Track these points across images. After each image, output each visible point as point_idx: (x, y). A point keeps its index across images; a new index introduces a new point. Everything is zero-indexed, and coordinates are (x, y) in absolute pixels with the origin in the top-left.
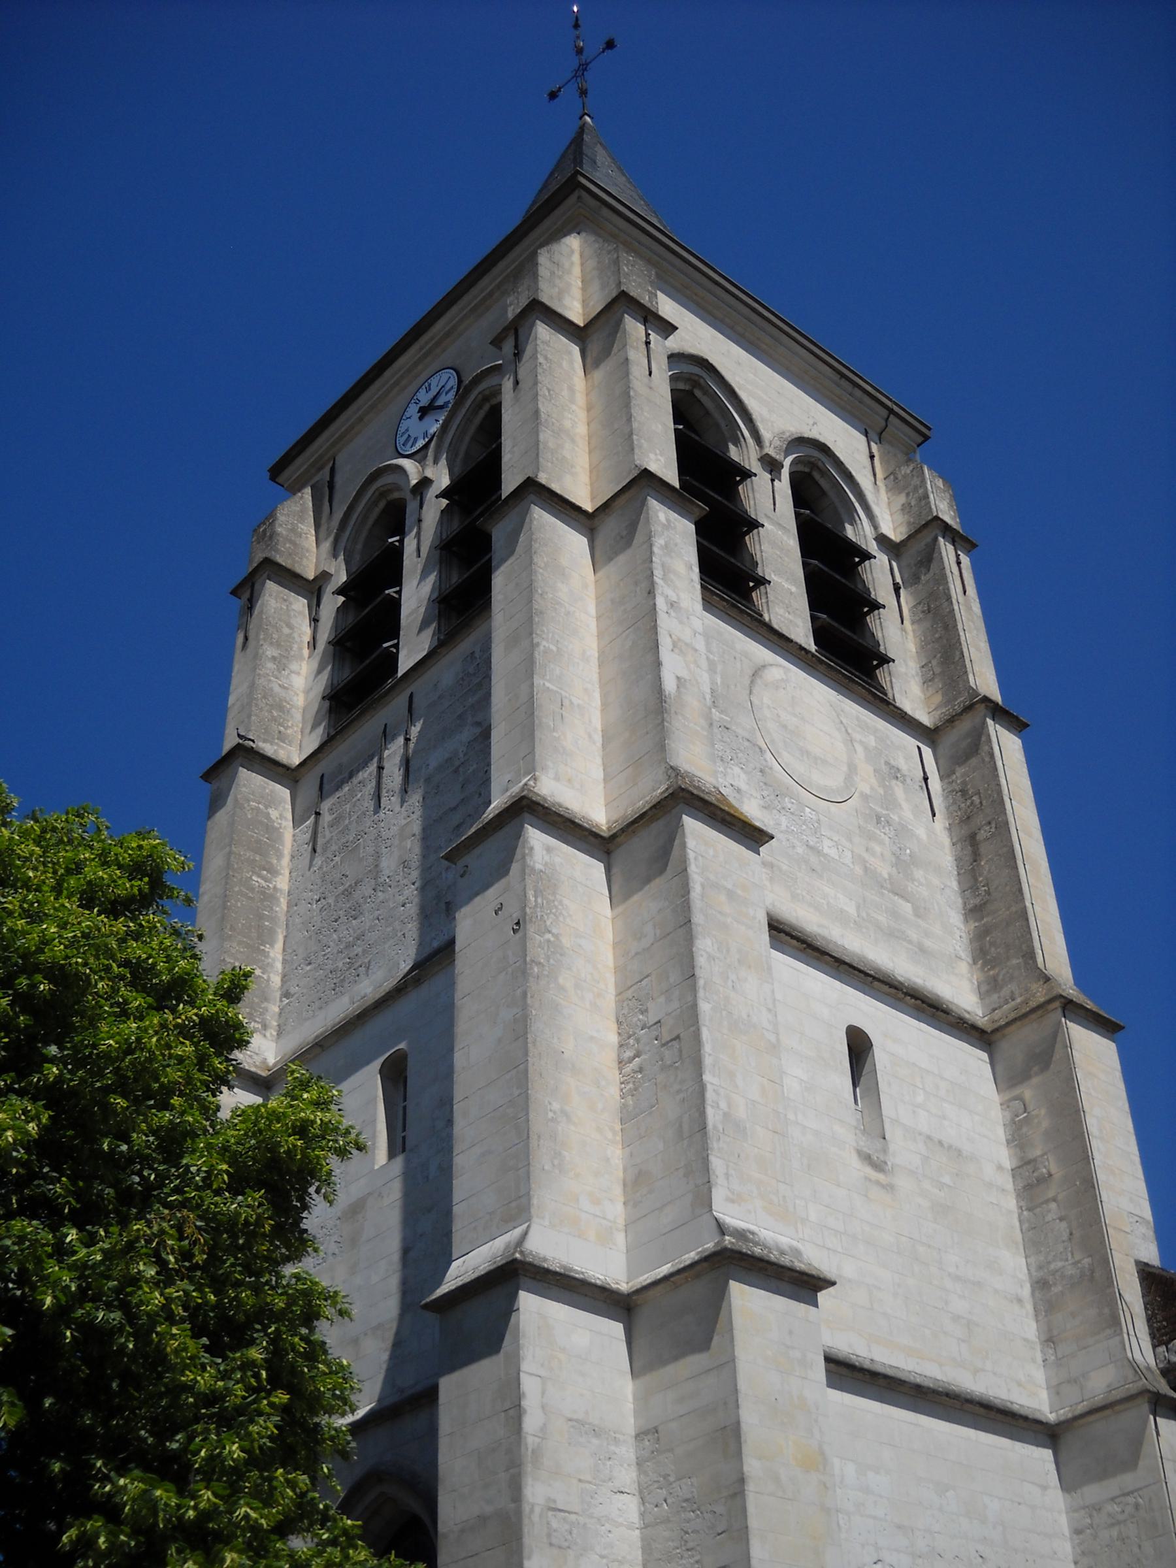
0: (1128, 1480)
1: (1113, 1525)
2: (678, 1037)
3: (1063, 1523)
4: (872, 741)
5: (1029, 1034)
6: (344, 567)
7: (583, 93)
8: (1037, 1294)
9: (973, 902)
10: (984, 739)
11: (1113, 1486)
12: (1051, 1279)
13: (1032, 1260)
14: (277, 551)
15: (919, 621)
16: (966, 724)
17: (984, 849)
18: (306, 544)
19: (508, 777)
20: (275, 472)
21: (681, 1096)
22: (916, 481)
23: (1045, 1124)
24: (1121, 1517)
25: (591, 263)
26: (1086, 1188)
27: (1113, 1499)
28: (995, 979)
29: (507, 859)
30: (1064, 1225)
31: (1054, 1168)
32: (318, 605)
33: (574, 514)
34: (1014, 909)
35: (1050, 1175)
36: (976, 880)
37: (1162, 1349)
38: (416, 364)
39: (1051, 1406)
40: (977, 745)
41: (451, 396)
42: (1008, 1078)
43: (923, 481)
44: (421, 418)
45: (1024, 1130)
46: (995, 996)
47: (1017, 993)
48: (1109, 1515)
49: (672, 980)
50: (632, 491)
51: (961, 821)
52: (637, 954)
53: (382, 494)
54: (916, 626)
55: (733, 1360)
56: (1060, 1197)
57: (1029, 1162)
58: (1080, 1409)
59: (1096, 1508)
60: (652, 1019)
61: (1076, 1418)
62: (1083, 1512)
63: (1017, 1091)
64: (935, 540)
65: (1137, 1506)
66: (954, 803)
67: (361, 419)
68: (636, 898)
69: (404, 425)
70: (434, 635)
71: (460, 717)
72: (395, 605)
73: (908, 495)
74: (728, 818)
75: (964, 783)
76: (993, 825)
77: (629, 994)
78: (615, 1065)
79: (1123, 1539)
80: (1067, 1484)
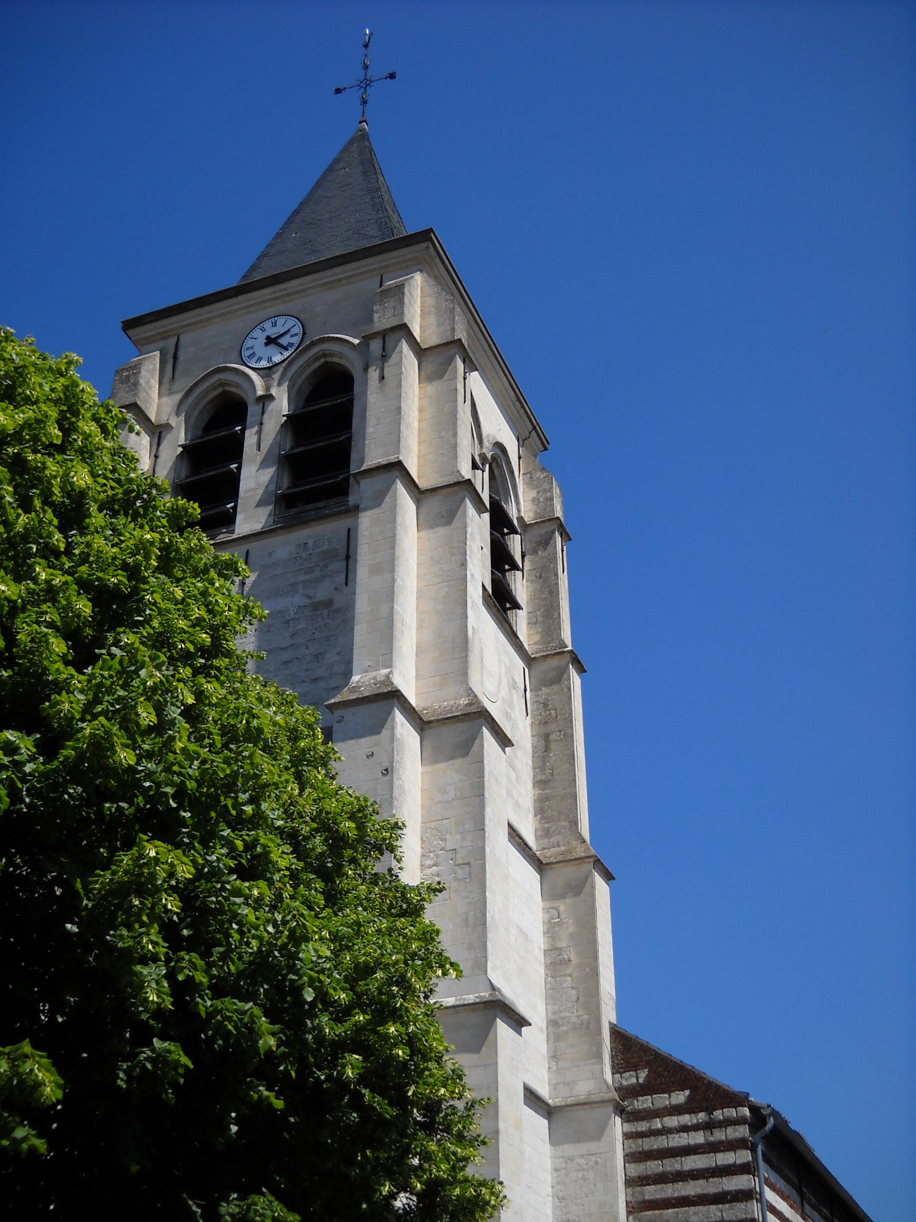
0: (593, 1146)
1: (579, 1170)
2: (468, 864)
3: (548, 1163)
4: (507, 661)
5: (569, 872)
6: (183, 425)
7: (365, 102)
8: (550, 1028)
9: (540, 777)
10: (565, 676)
11: (583, 1148)
12: (560, 1021)
13: (549, 1007)
14: (139, 397)
15: (532, 581)
16: (555, 662)
17: (553, 746)
18: (152, 395)
19: (369, 663)
20: (128, 325)
21: (469, 900)
22: (546, 486)
23: (571, 929)
24: (585, 1167)
25: (430, 301)
26: (594, 974)
27: (582, 1156)
28: (548, 830)
29: (378, 725)
30: (574, 992)
31: (572, 957)
32: (159, 445)
33: (413, 488)
34: (568, 791)
35: (570, 961)
36: (545, 764)
37: (618, 1076)
38: (266, 301)
39: (550, 1094)
40: (560, 678)
41: (296, 340)
42: (550, 894)
43: (551, 488)
44: (266, 344)
45: (557, 929)
46: (546, 841)
47: (561, 843)
48: (578, 1164)
49: (466, 827)
50: (456, 489)
51: (540, 723)
52: (440, 802)
53: (222, 384)
54: (529, 584)
55: (496, 1064)
56: (574, 975)
57: (556, 949)
58: (570, 1101)
59: (571, 1159)
60: (449, 847)
61: (567, 1106)
62: (561, 1160)
63: (555, 904)
64: (553, 532)
65: (596, 1163)
66: (538, 709)
67: (210, 319)
68: (442, 765)
69: (249, 343)
70: (270, 515)
71: (292, 585)
72: (234, 480)
73: (538, 492)
74: (499, 731)
75: (547, 699)
76: (563, 733)
77: (433, 825)
78: (419, 867)
79: (584, 1179)
80: (554, 1140)
